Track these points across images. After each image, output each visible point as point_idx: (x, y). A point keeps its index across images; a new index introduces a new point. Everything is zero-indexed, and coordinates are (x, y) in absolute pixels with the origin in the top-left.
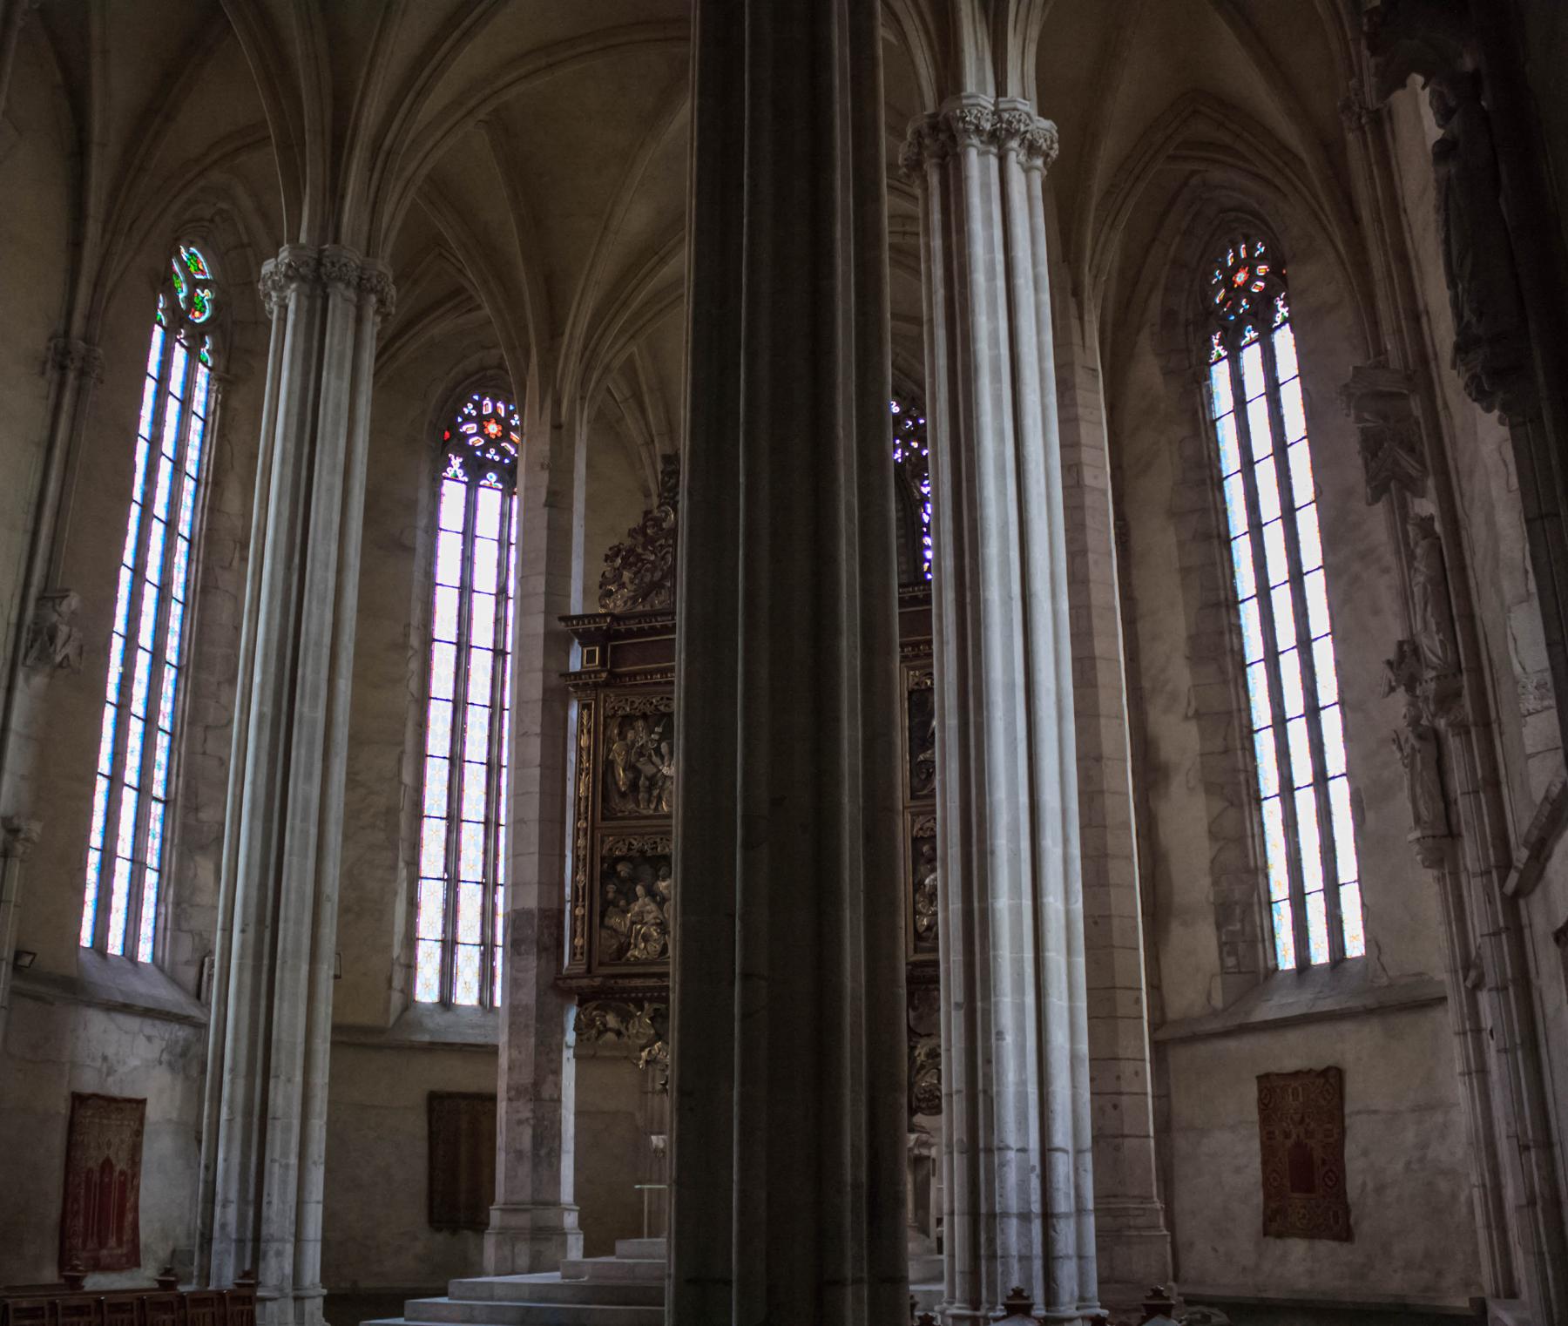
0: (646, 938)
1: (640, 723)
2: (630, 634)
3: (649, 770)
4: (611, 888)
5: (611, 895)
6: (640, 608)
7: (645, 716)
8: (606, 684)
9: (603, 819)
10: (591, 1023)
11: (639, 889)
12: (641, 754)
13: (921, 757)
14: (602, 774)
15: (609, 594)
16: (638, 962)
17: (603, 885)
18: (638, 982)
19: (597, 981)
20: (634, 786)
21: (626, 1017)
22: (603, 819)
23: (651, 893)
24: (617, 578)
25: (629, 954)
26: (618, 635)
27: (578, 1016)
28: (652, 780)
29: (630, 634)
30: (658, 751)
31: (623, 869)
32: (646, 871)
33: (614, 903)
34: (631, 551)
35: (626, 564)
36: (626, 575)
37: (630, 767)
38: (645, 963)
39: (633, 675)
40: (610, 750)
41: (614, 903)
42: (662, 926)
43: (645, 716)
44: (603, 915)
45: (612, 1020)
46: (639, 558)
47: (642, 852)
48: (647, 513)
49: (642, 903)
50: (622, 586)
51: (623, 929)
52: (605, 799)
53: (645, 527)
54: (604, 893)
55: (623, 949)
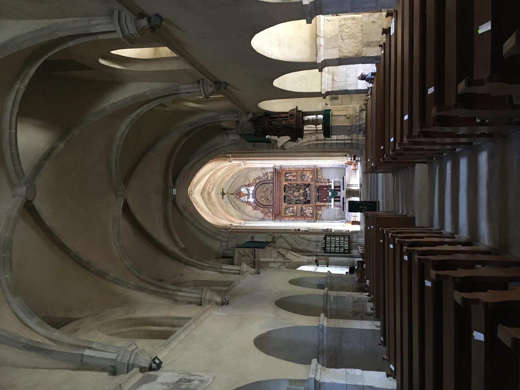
0: (310, 211)
1: (286, 212)
2: (275, 213)
3: (291, 211)
4: (304, 215)
5: (305, 215)
6: (272, 213)
7: (285, 211)
8: (281, 216)
9: (296, 216)
10: (319, 218)
11: (305, 212)
12: (289, 212)
13: (292, 180)
14: (291, 216)
15: (270, 216)
16: (313, 212)
17: (303, 216)
18: (315, 212)
19: (315, 216)
20: (293, 213)
21: (319, 214)
22: (296, 216)
23: (305, 211)
24: (268, 215)
25: (312, 213)
26: (275, 215)
27: (318, 220)
28: (293, 210)
29: (275, 213)
30: (289, 210)
31: (302, 214)
32: (303, 211)
33: (306, 215)
34: (265, 214)
35: (266, 214)
36: (268, 214)
37: (291, 213)
38: (313, 211)
39: (280, 213)
40: (289, 215)
41: (306, 215)
42: (309, 209)
43: (285, 211)
44: (307, 216)
45: (319, 216)
46: (266, 213)
47: (301, 211)
48: (260, 212)
49: (306, 211)
50: (269, 215)
51: (309, 214)
52: (294, 216)
53: (262, 212)
54: (305, 216)
55: (311, 214)
